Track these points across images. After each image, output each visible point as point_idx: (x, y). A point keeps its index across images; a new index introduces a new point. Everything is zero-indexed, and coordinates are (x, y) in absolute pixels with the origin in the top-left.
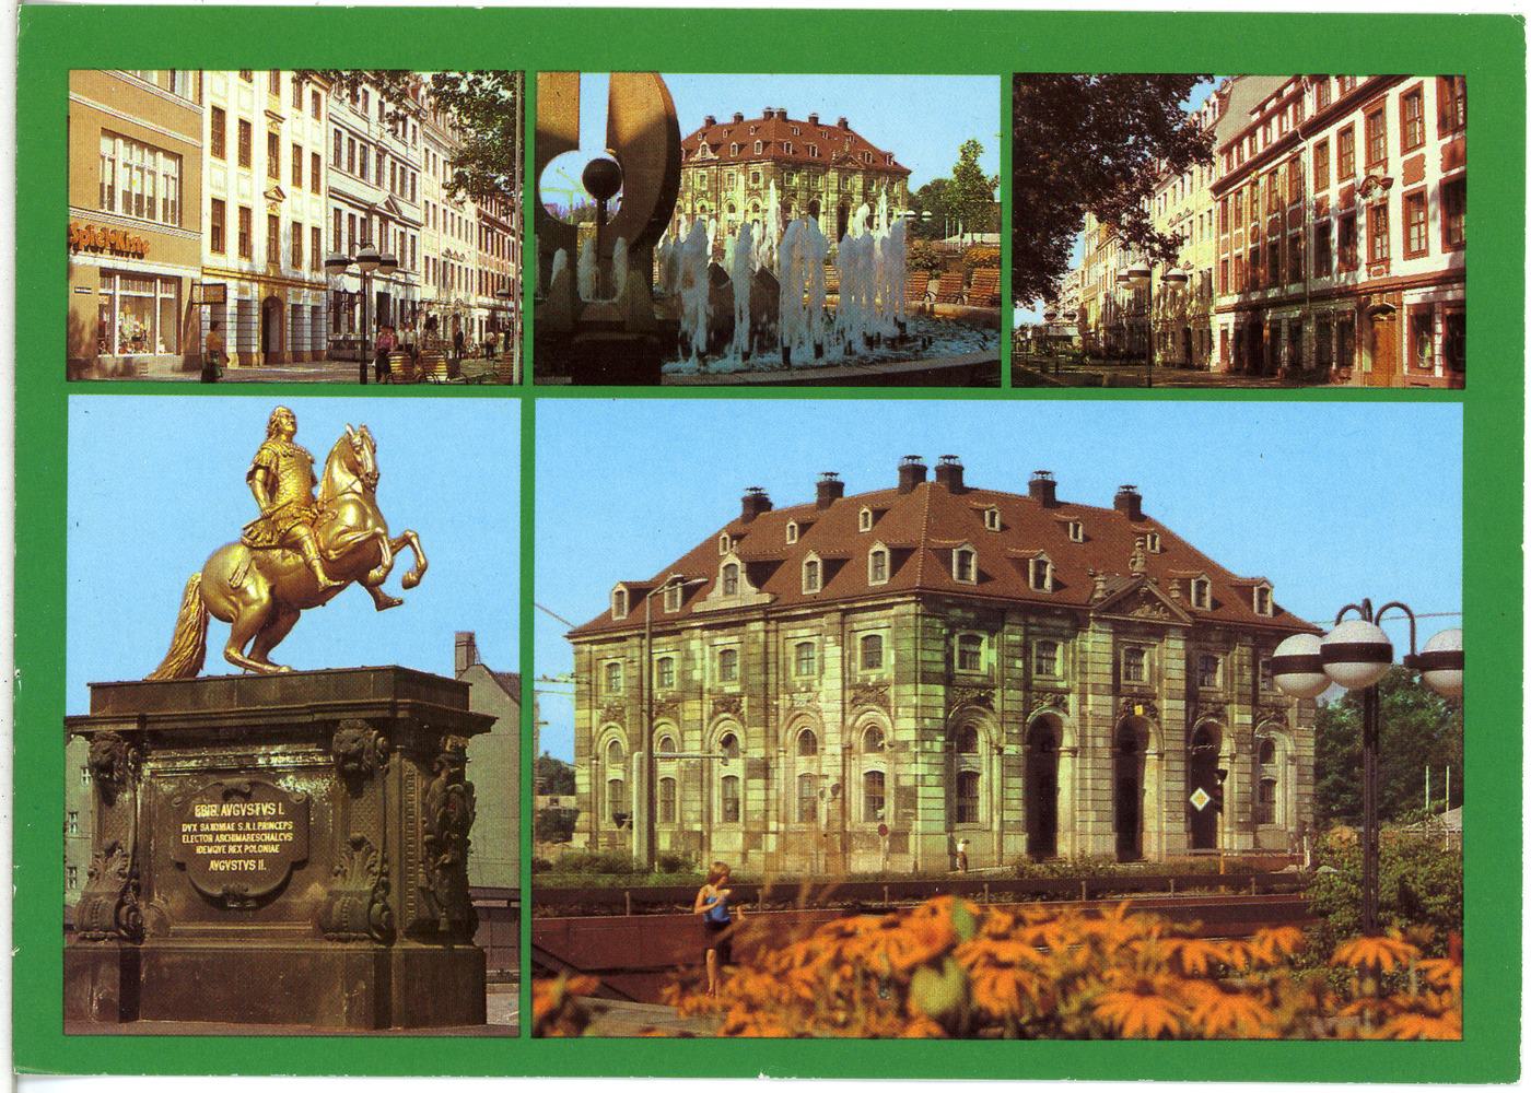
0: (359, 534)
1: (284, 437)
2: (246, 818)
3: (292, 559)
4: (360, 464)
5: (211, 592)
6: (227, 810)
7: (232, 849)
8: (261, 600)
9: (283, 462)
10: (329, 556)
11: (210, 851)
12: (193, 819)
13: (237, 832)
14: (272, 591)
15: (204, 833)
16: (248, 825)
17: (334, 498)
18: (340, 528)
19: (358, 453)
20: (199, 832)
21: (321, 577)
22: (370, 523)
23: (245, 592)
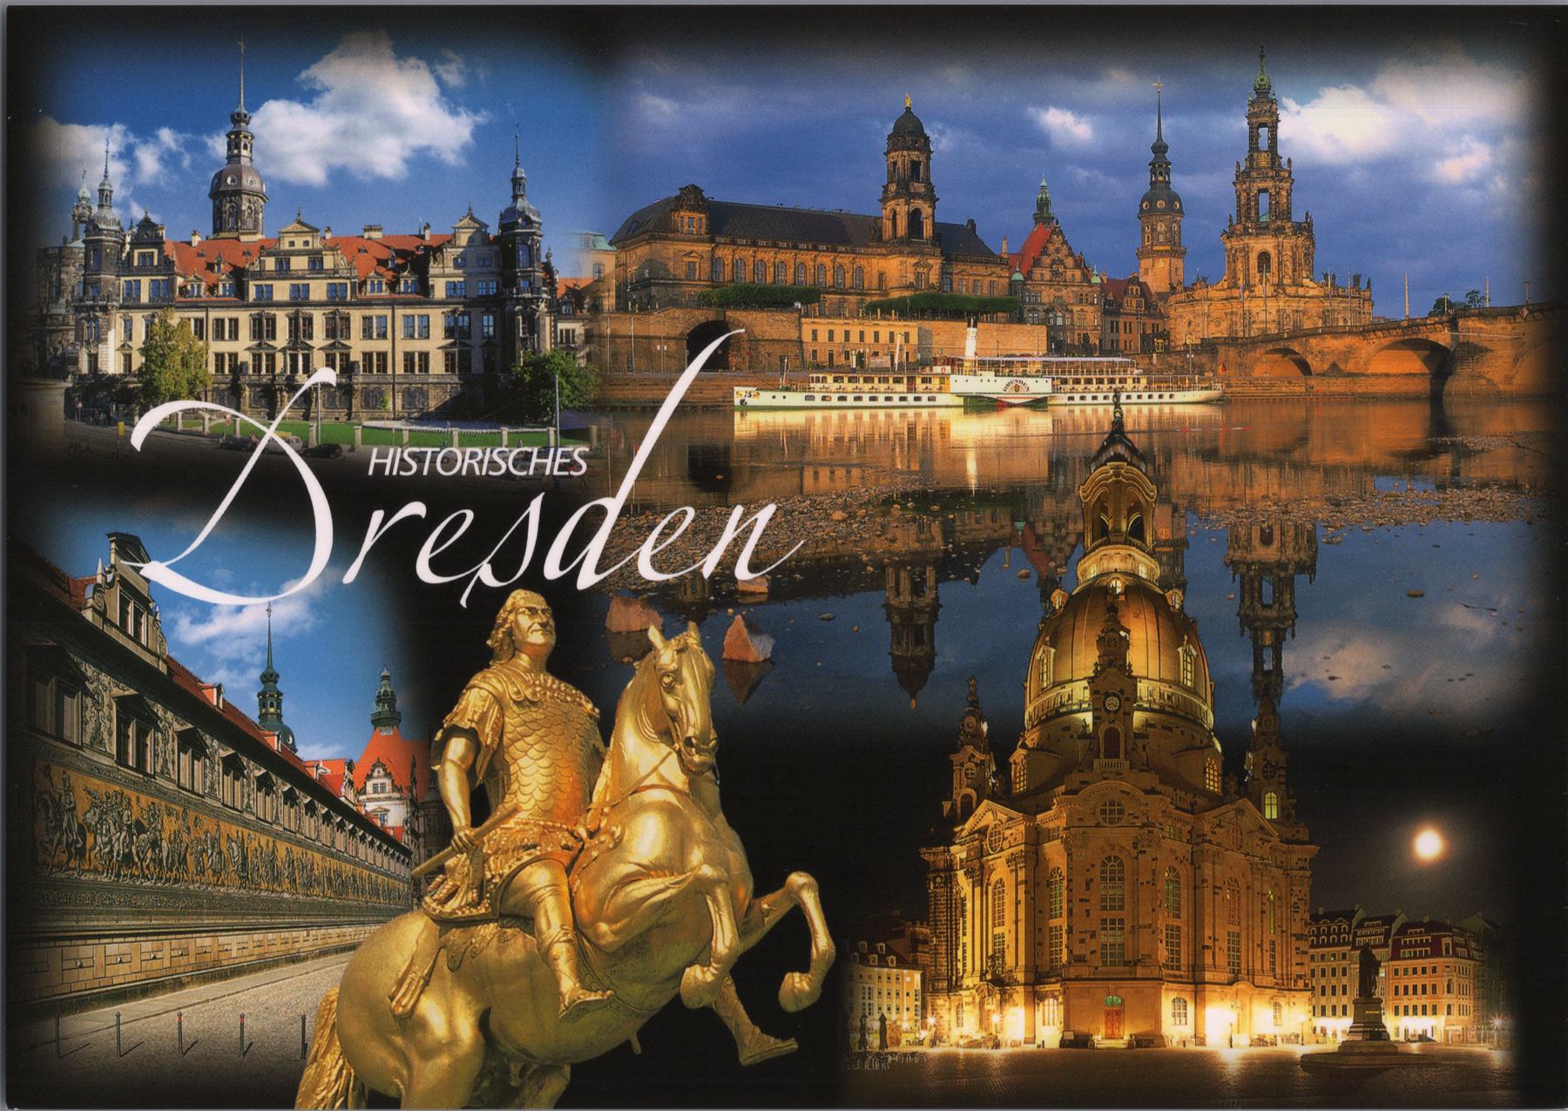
0: (668, 880)
1: (524, 660)
3: (518, 946)
4: (674, 717)
5: (354, 1028)
8: (454, 1040)
9: (512, 721)
10: (598, 936)
14: (483, 1023)
17: (629, 792)
18: (625, 869)
19: (670, 689)
21: (568, 984)
22: (696, 855)
23: (423, 1025)
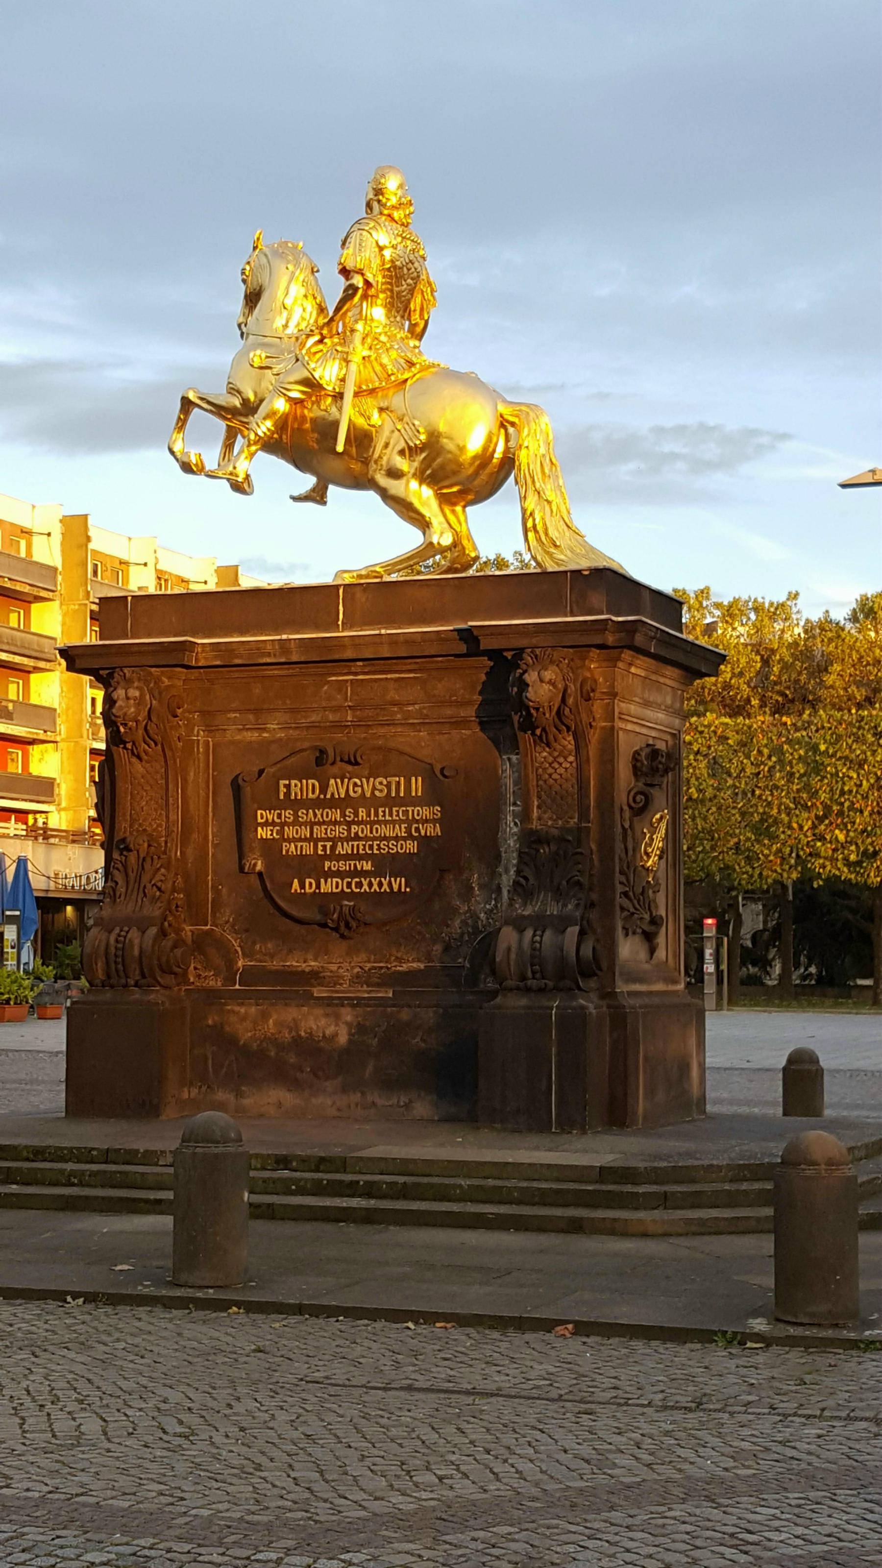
6: (337, 788)
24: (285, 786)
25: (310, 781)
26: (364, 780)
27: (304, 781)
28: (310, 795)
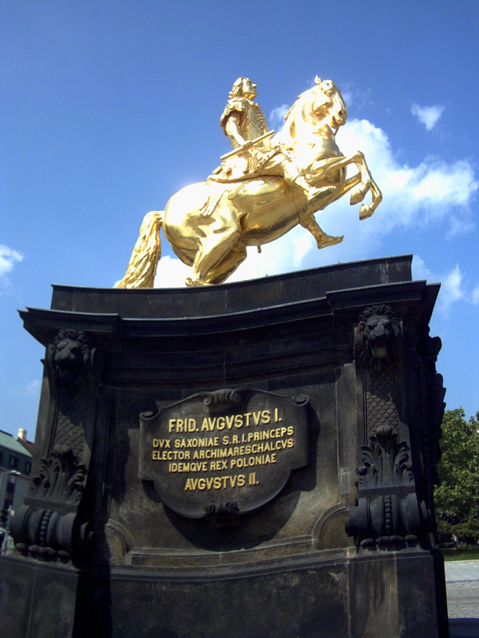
2: (230, 432)
6: (208, 424)
7: (214, 466)
11: (186, 468)
12: (165, 435)
13: (221, 446)
15: (179, 449)
16: (235, 438)
20: (172, 448)
24: (173, 423)
25: (190, 420)
26: (227, 417)
27: (186, 420)
28: (190, 430)
